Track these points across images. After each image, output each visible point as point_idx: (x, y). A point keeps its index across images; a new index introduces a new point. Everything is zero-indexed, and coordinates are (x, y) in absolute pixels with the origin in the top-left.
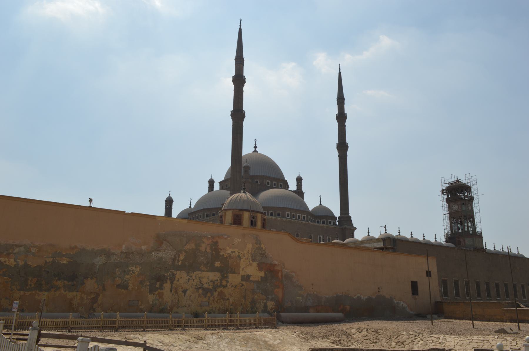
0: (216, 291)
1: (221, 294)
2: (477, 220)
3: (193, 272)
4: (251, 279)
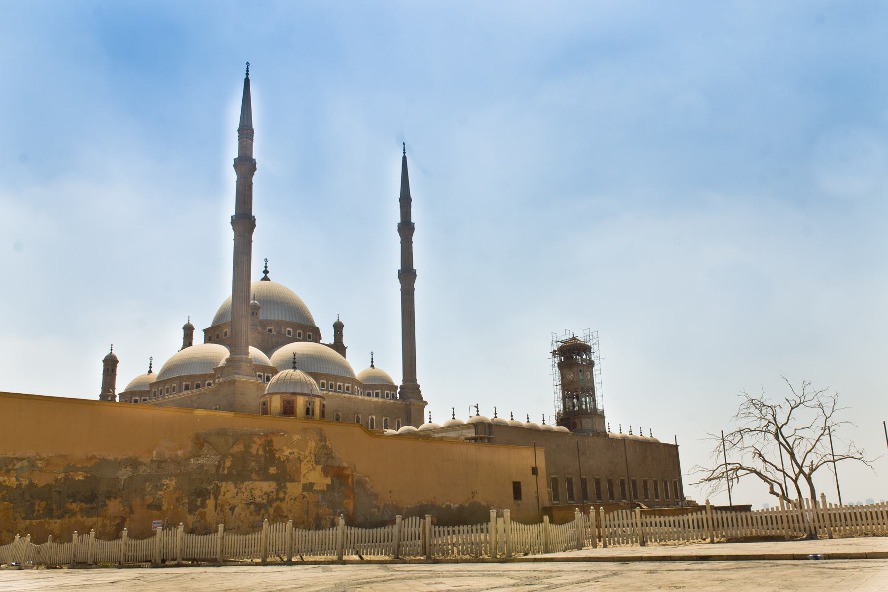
1: (278, 509)
2: (597, 393)
3: (243, 482)
4: (315, 488)
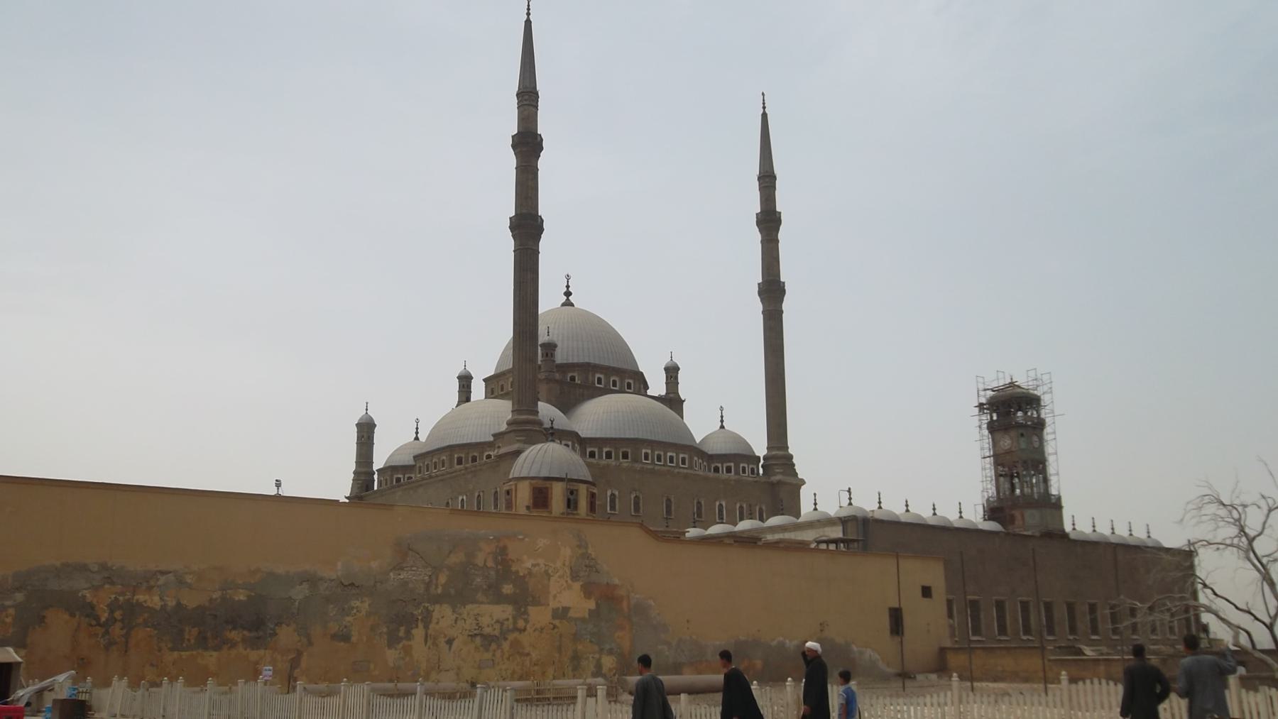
0: (506, 639)
1: (516, 644)
2: (1051, 470)
3: (464, 605)
4: (571, 614)
